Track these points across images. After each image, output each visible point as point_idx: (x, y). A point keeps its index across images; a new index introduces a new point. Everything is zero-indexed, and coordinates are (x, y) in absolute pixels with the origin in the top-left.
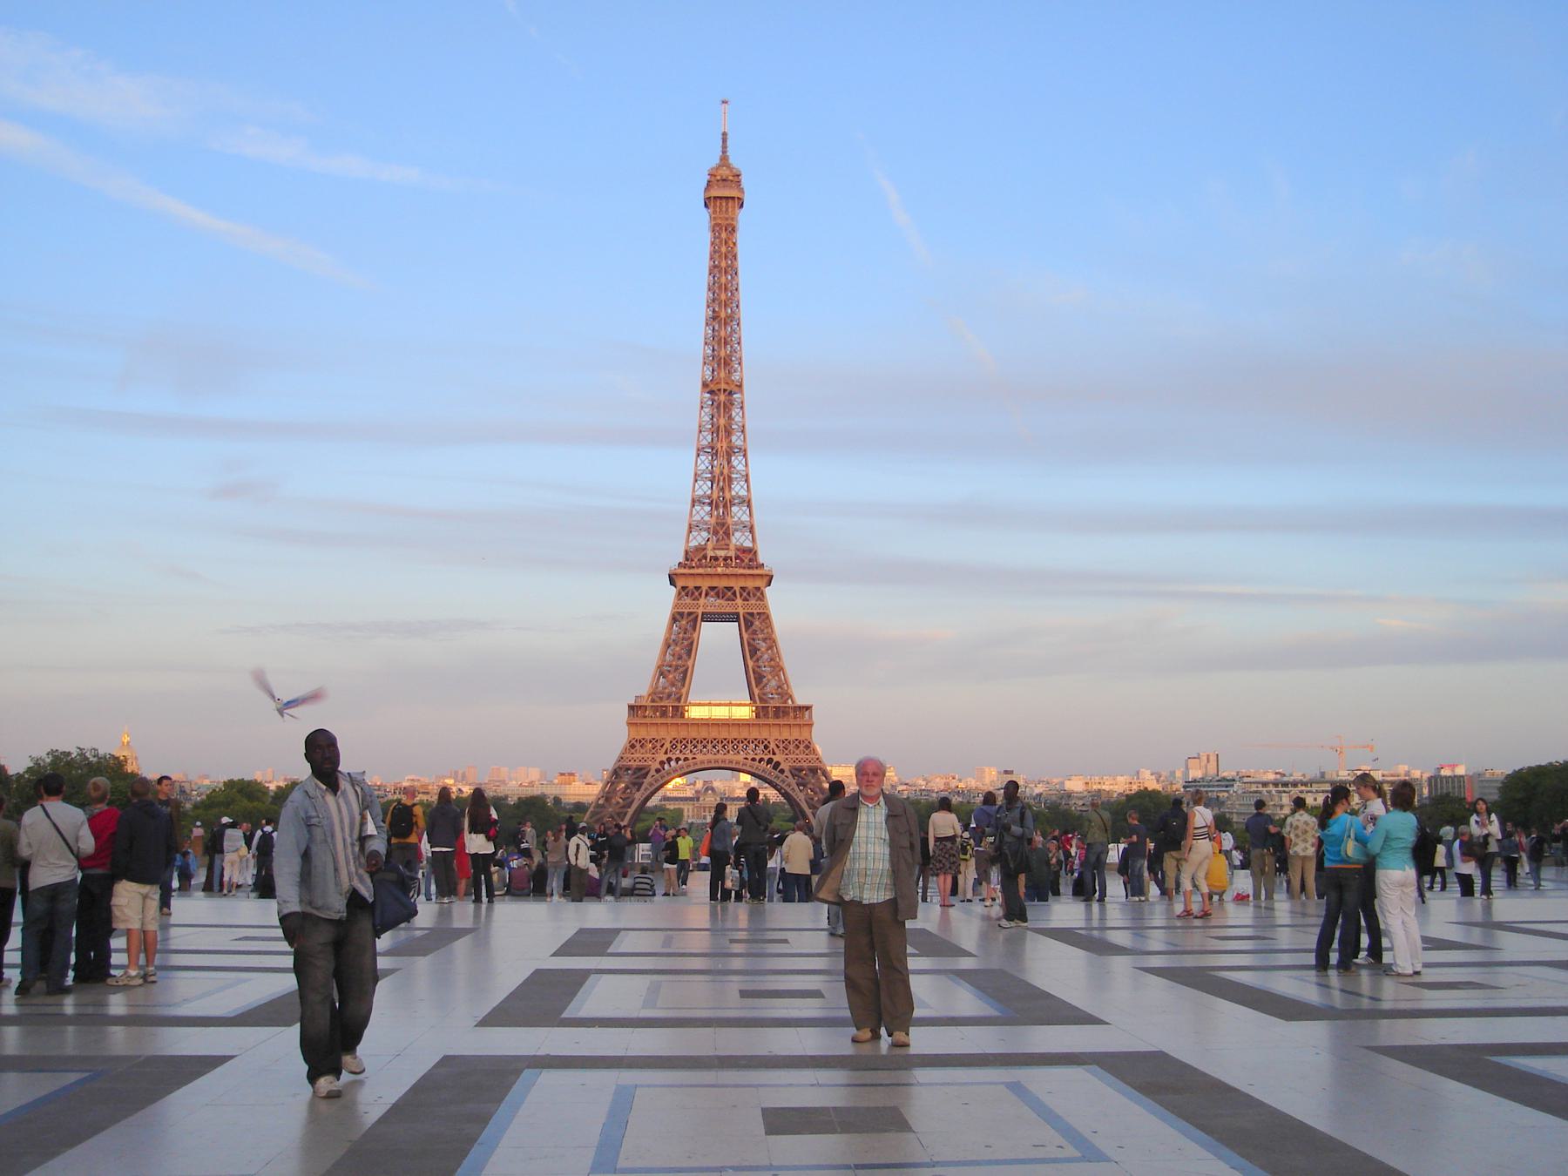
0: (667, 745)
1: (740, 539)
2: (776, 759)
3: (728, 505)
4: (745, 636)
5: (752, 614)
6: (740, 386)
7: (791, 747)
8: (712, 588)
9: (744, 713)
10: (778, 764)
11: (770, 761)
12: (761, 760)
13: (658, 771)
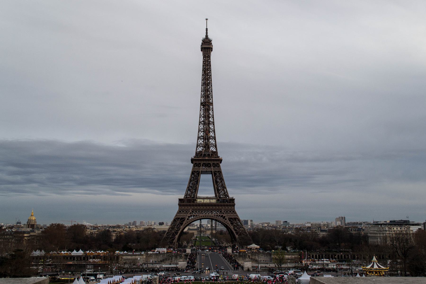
0: (191, 211)
1: (212, 149)
2: (224, 215)
3: (208, 139)
4: (214, 178)
5: (216, 171)
6: (212, 104)
7: (229, 212)
8: (204, 164)
9: (214, 201)
10: (224, 217)
11: (222, 216)
12: (220, 216)
13: (188, 219)
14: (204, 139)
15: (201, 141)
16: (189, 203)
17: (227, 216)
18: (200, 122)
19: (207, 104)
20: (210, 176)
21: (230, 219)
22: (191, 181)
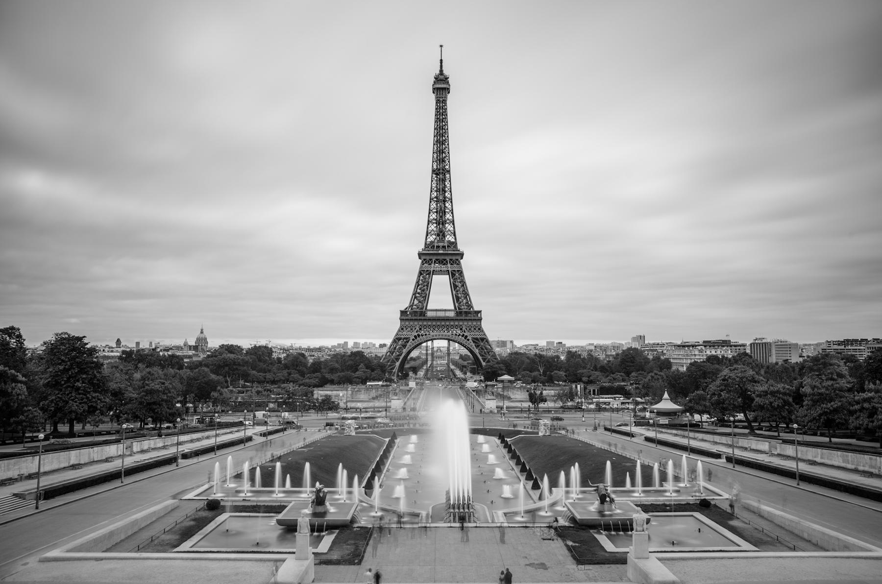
3: (444, 223)
9: (452, 314)
14: (438, 223)
15: (433, 227)
16: (416, 317)
18: (431, 199)
19: (441, 173)
20: (446, 278)
21: (475, 340)
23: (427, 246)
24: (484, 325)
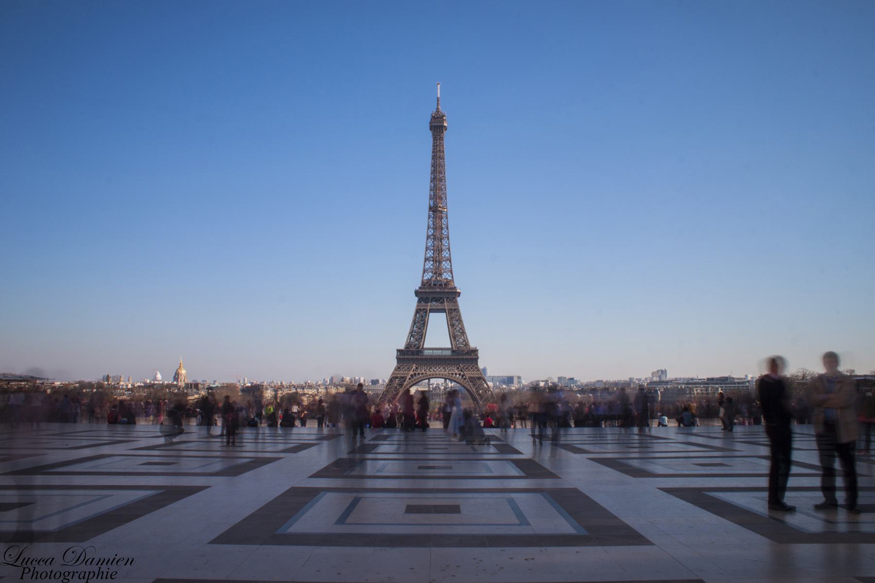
0: (414, 367)
1: (446, 276)
9: (449, 353)
14: (435, 261)
15: (429, 265)
17: (468, 374)
18: (428, 237)
19: (436, 211)
22: (414, 322)
23: (423, 284)
24: (481, 365)
